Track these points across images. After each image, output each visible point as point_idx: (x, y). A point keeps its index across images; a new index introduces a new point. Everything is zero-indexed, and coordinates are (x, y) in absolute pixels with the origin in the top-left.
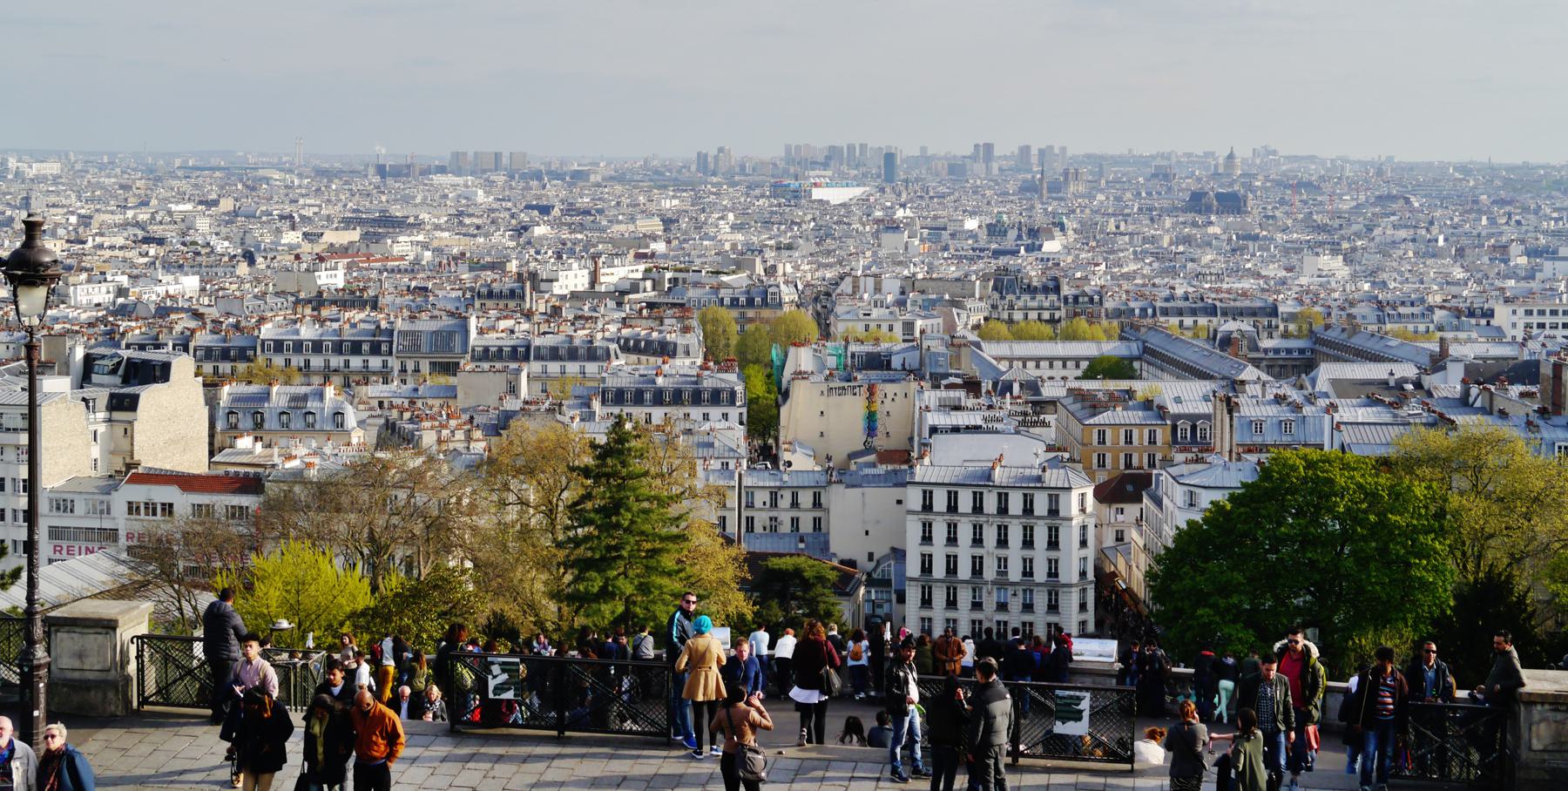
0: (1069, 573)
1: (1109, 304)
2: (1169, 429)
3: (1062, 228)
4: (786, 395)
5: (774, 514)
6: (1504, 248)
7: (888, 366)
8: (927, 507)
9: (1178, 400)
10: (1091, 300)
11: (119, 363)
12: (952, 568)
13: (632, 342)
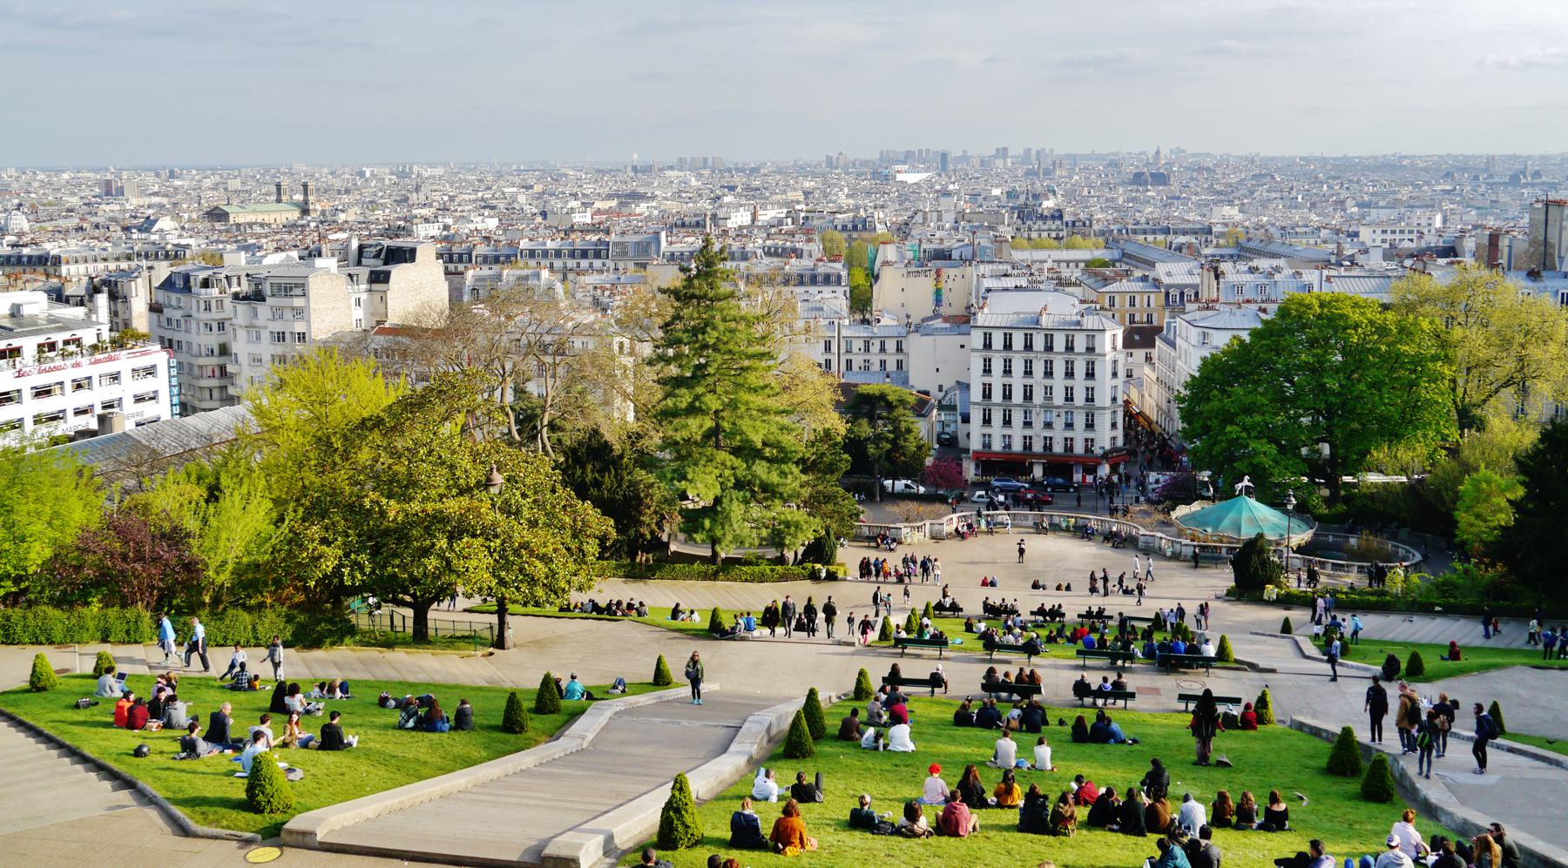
0: (1103, 398)
1: (1096, 227)
2: (1163, 296)
3: (1054, 193)
4: (877, 278)
5: (867, 357)
6: (1342, 202)
7: (950, 258)
8: (988, 346)
9: (1169, 274)
10: (1084, 224)
11: (381, 250)
12: (1007, 395)
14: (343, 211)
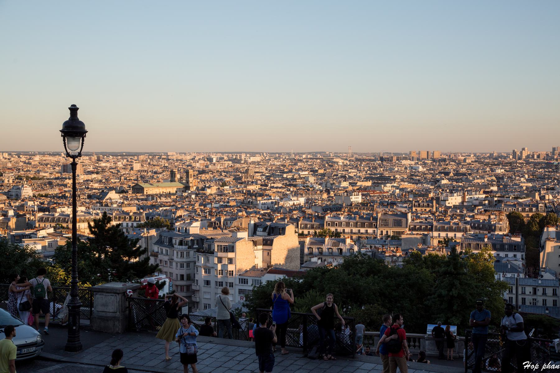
5: (535, 297)
13: (476, 225)
14: (209, 187)
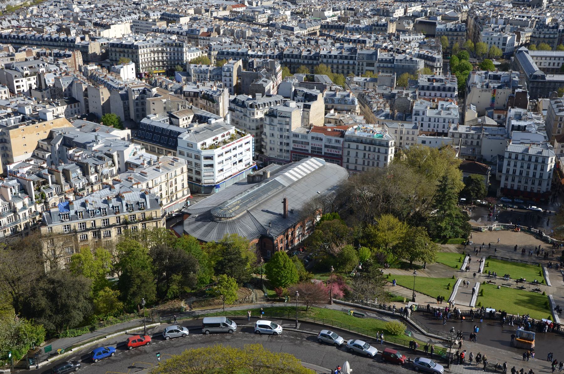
12: (514, 172)
